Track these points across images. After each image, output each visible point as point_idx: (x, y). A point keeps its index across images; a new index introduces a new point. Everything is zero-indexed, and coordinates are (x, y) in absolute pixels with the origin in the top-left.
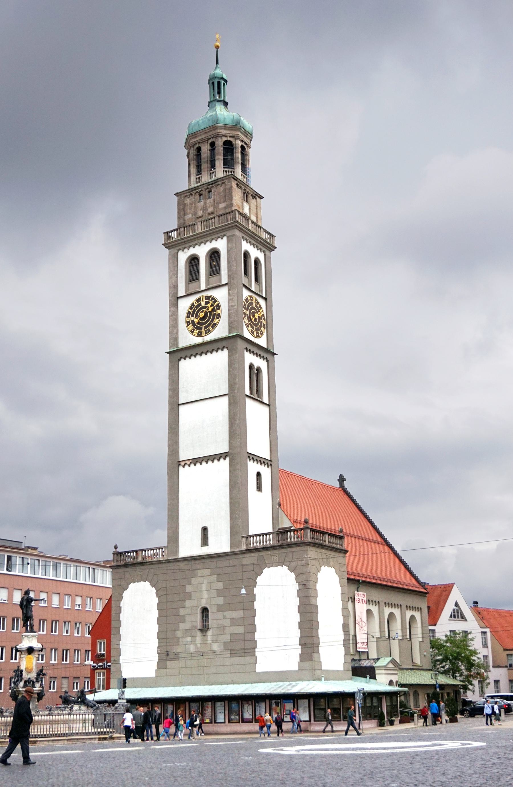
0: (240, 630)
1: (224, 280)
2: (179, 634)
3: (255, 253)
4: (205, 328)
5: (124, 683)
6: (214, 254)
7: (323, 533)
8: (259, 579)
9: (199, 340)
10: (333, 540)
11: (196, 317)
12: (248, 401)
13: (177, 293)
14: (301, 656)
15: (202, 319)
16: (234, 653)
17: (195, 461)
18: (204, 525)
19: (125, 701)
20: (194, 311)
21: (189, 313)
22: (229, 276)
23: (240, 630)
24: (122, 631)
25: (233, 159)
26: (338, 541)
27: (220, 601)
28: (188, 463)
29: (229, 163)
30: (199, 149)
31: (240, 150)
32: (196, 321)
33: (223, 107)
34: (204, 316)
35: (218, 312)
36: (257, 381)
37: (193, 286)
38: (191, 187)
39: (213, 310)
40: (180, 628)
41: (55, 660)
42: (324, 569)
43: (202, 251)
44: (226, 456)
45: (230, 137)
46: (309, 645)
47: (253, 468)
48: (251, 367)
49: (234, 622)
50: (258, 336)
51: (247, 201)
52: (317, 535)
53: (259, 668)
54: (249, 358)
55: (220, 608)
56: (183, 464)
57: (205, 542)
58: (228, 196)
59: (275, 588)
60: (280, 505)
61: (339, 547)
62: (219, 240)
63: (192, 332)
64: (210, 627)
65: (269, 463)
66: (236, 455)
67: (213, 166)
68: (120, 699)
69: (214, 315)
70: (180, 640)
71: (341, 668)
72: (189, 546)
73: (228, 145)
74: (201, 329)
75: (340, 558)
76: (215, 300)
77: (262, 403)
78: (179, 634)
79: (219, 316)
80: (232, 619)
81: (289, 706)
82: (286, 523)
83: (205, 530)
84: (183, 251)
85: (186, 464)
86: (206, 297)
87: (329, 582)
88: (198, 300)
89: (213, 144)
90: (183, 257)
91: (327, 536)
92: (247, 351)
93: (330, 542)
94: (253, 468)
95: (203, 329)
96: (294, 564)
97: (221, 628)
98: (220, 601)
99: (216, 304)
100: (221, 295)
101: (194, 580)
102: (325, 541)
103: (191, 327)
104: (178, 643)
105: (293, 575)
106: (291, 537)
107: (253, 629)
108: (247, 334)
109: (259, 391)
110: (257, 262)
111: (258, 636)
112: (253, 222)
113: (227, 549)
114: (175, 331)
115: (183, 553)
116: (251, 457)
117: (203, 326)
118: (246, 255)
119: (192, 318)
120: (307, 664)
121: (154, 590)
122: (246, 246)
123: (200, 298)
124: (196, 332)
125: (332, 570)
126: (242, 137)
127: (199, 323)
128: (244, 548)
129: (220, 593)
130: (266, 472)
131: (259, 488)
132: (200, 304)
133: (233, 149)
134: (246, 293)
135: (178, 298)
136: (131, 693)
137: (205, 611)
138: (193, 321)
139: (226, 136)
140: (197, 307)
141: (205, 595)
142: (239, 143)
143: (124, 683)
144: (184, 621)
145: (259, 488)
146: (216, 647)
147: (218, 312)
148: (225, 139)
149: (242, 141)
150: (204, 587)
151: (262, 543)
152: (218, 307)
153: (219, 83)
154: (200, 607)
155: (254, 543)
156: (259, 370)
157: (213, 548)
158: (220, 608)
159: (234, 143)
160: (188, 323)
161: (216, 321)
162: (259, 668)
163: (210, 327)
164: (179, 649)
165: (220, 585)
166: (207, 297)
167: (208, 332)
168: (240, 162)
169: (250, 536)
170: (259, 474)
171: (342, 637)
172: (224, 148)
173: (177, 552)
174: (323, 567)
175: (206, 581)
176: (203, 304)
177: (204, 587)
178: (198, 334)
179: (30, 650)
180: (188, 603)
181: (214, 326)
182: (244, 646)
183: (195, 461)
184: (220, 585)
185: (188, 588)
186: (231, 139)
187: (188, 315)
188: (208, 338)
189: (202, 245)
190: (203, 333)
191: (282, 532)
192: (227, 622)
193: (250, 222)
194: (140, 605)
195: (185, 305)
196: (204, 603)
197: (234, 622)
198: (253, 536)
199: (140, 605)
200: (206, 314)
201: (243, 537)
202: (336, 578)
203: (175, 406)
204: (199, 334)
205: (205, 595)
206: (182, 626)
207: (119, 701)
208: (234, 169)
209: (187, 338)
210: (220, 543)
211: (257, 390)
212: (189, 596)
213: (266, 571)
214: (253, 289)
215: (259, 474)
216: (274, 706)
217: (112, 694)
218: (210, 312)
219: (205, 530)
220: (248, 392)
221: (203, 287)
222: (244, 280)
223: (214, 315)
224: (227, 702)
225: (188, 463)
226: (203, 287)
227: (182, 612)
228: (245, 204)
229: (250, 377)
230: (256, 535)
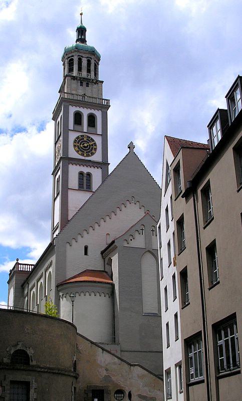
15: (85, 147)
20: (79, 141)
37: (78, 127)
43: (85, 112)
63: (77, 152)
69: (92, 148)
79: (95, 149)
86: (87, 136)
90: (73, 110)
100: (98, 140)
103: (76, 148)
124: (80, 152)
140: (81, 139)
160: (75, 146)
161: (93, 151)
167: (88, 156)
181: (93, 154)
187: (75, 141)
190: (85, 155)
195: (73, 136)
204: (83, 155)
209: (73, 153)
221: (85, 130)
223: (92, 148)
226: (85, 130)
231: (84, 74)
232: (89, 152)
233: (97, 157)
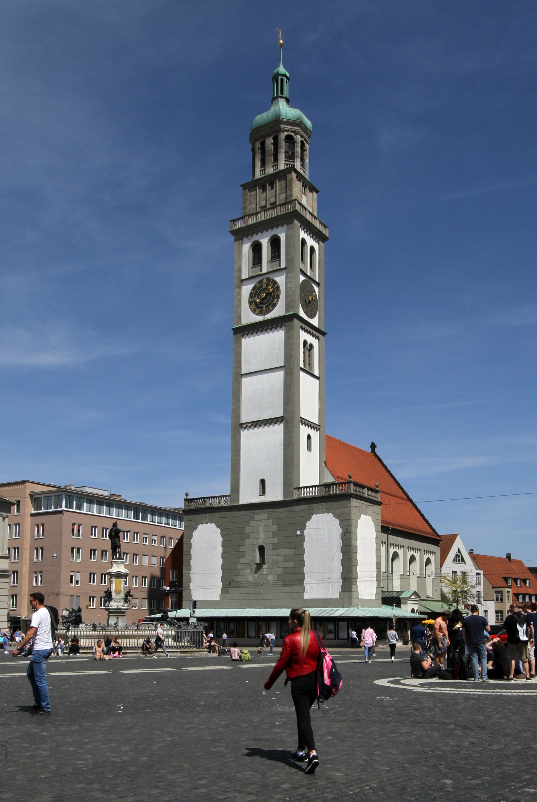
0: (291, 564)
1: (283, 265)
2: (239, 566)
3: (310, 242)
4: (266, 307)
5: (195, 605)
6: (275, 242)
7: (363, 487)
8: (308, 524)
9: (260, 318)
10: (370, 493)
11: (258, 298)
12: (302, 374)
13: (241, 276)
14: (342, 587)
15: (263, 299)
16: (286, 583)
17: (256, 424)
18: (262, 478)
19: (196, 619)
20: (256, 292)
21: (251, 294)
22: (287, 261)
23: (291, 564)
24: (192, 563)
25: (293, 153)
26: (375, 494)
27: (275, 540)
28: (249, 425)
29: (290, 157)
30: (263, 144)
31: (299, 144)
32: (258, 301)
33: (285, 103)
34: (264, 297)
35: (277, 293)
36: (309, 356)
38: (255, 179)
39: (273, 291)
40: (241, 562)
41: (136, 585)
42: (363, 516)
44: (282, 420)
45: (292, 132)
46: (348, 579)
47: (305, 431)
48: (305, 342)
49: (286, 558)
50: (312, 316)
51: (304, 194)
52: (358, 489)
53: (306, 596)
54: (304, 336)
55: (275, 547)
56: (244, 426)
57: (263, 493)
58: (288, 188)
59: (321, 530)
60: (325, 463)
61: (375, 499)
62: (280, 228)
63: (254, 311)
64: (266, 561)
65: (318, 427)
66: (289, 419)
67: (276, 159)
68: (191, 617)
69: (274, 296)
70: (241, 571)
71: (374, 598)
72: (249, 495)
73: (290, 139)
74: (262, 308)
75: (377, 509)
76: (275, 282)
77: (313, 375)
78: (239, 566)
79: (278, 297)
80: (284, 556)
81: (331, 627)
82: (330, 479)
83: (263, 482)
84: (247, 237)
85: (247, 426)
87: (366, 527)
88: (260, 282)
89: (276, 139)
91: (366, 489)
92: (302, 330)
93: (368, 495)
94: (305, 431)
95: (264, 308)
96: (338, 512)
97: (275, 562)
98: (275, 540)
99: (276, 286)
100: (281, 280)
101: (253, 524)
102: (364, 494)
103: (253, 306)
104: (238, 574)
105: (337, 521)
106: (334, 490)
107: (302, 564)
108: (302, 314)
109: (311, 365)
110: (312, 249)
111: (306, 570)
112: (310, 213)
113: (279, 497)
114: (239, 310)
115: (244, 500)
116: (303, 421)
117: (264, 306)
118: (304, 242)
119: (254, 299)
120: (346, 594)
121: (219, 530)
122: (303, 234)
123: (261, 281)
124: (258, 311)
125: (369, 518)
126: (302, 133)
127: (261, 303)
128: (295, 497)
129: (274, 534)
130: (315, 435)
131: (309, 448)
132: (262, 286)
133: (294, 143)
134: (302, 278)
135: (242, 281)
136: (200, 613)
137: (262, 549)
138: (255, 301)
139: (288, 131)
140: (259, 289)
141: (262, 535)
142: (298, 138)
143: (195, 605)
144: (244, 557)
145: (309, 448)
146: (270, 578)
147: (277, 293)
148: (286, 133)
149: (302, 136)
150: (261, 529)
151: (311, 494)
152: (278, 288)
153: (282, 80)
154: (258, 545)
155: (305, 493)
156: (311, 346)
157: (269, 497)
158: (275, 547)
159: (295, 137)
160: (250, 303)
162: (306, 596)
163: (271, 308)
164: (239, 579)
165: (275, 528)
166: (268, 280)
167: (268, 311)
168: (300, 156)
169: (301, 488)
170: (309, 437)
171: (375, 574)
172: (285, 142)
173: (238, 500)
174: (362, 515)
175: (263, 524)
176: (264, 286)
177: (261, 529)
178: (259, 313)
179: (118, 575)
180: (247, 542)
181: (274, 305)
182: (294, 577)
183: (256, 424)
184: (275, 528)
185: (248, 530)
186: (293, 134)
187: (251, 295)
188: (268, 316)
189: (265, 232)
190: (264, 312)
191: (328, 486)
192: (281, 558)
193: (307, 212)
194: (207, 543)
196: (261, 542)
197: (286, 558)
198: (304, 488)
199: (207, 543)
200: (267, 295)
201: (295, 489)
202: (372, 525)
203: (238, 376)
204: (261, 314)
205: (262, 535)
206: (242, 560)
207: (190, 618)
208: (294, 162)
210: (275, 494)
211: (309, 364)
212: (247, 536)
213: (314, 517)
214: (309, 274)
215: (309, 437)
216: (318, 626)
217: (183, 613)
218: (270, 293)
219: (263, 482)
220: (302, 365)
222: (301, 265)
223: (274, 296)
224: (279, 622)
225: (249, 425)
226: (264, 270)
227: (242, 549)
228: (303, 195)
229: (304, 353)
230: (307, 487)
231: (270, 170)
232: (270, 304)
233: (279, 311)
